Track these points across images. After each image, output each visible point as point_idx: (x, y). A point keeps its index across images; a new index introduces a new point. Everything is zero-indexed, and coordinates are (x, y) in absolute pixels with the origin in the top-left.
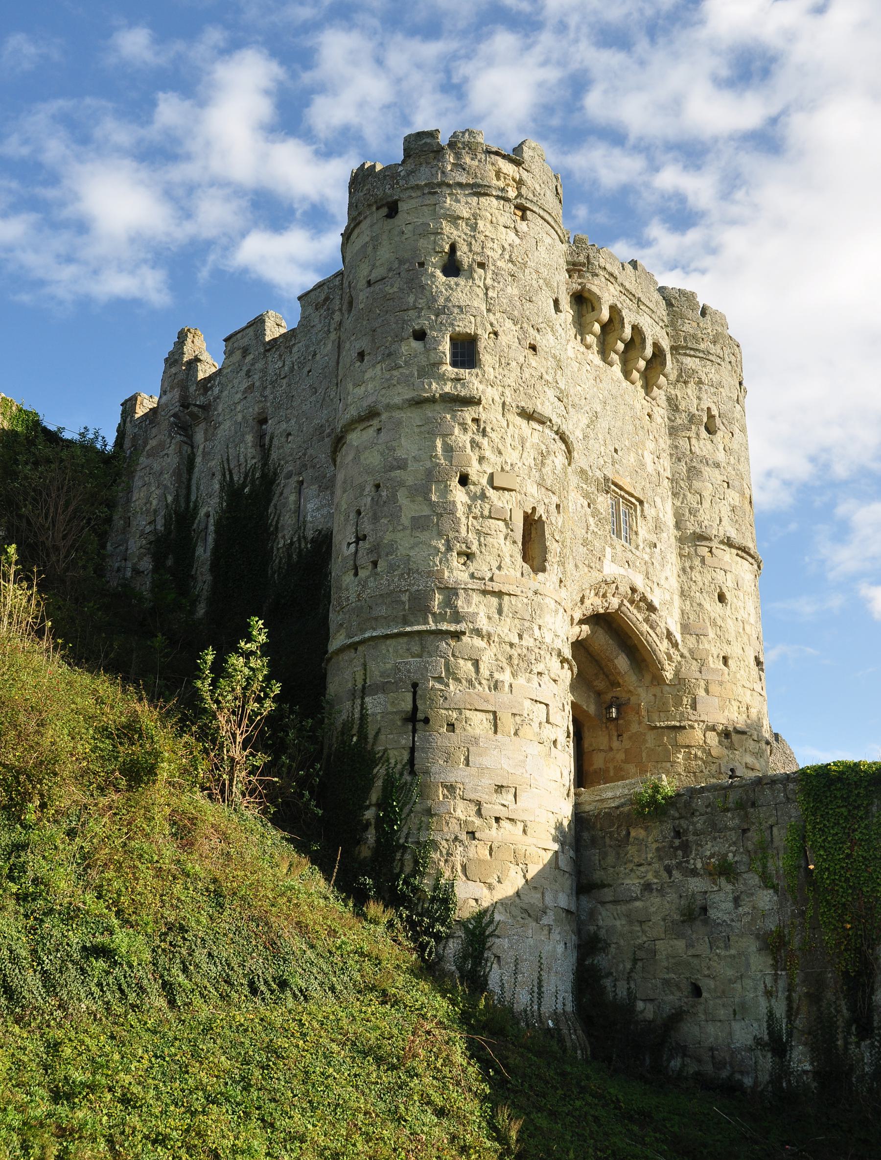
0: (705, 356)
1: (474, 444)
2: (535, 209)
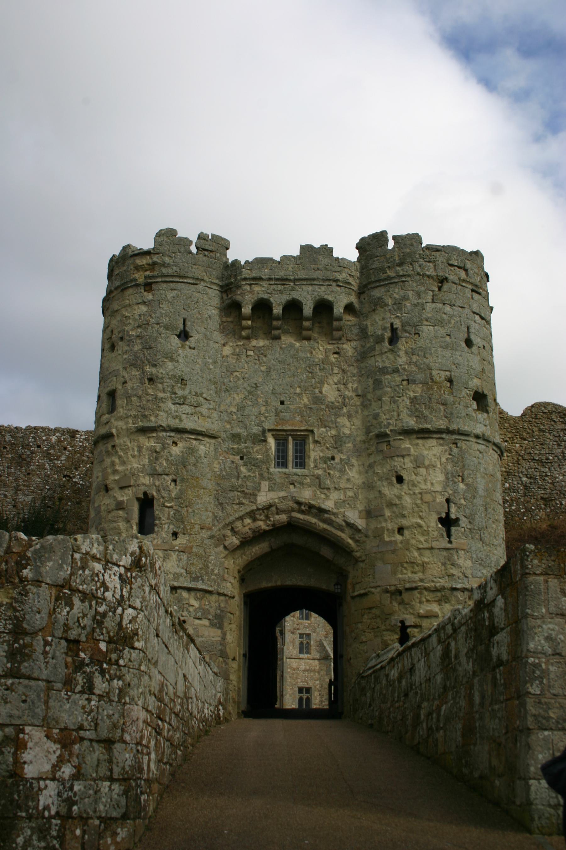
0: (389, 282)
1: (113, 464)
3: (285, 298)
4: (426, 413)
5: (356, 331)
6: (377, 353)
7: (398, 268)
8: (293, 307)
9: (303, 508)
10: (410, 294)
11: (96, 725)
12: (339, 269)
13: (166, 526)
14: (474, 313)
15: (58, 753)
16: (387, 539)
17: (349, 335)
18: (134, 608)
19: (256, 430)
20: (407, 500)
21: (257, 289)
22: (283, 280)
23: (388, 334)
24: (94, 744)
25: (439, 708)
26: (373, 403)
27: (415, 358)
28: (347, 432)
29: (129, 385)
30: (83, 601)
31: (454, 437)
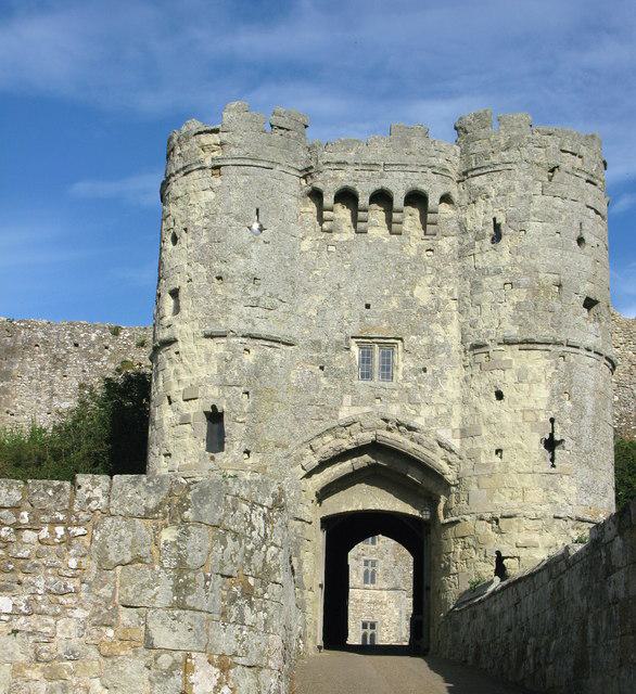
0: (493, 170)
1: (176, 372)
2: (229, 162)
3: (373, 187)
4: (531, 321)
5: (454, 225)
6: (476, 251)
7: (503, 153)
8: (382, 198)
9: (390, 425)
10: (517, 184)
11: (247, 652)
12: (435, 153)
13: (237, 443)
14: (588, 207)
15: (218, 675)
16: (483, 461)
17: (445, 231)
18: (276, 546)
19: (338, 336)
20: (507, 418)
21: (341, 175)
22: (371, 166)
23: (490, 230)
24: (246, 669)
25: (548, 643)
26: (471, 309)
27: (520, 259)
28: (442, 341)
29: (195, 284)
30: (234, 540)
31: (561, 349)
